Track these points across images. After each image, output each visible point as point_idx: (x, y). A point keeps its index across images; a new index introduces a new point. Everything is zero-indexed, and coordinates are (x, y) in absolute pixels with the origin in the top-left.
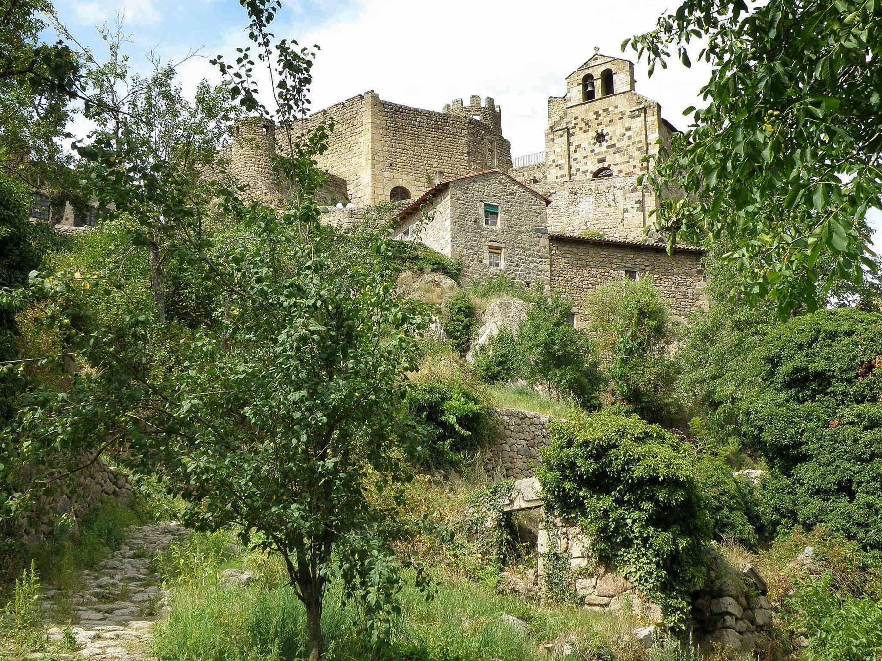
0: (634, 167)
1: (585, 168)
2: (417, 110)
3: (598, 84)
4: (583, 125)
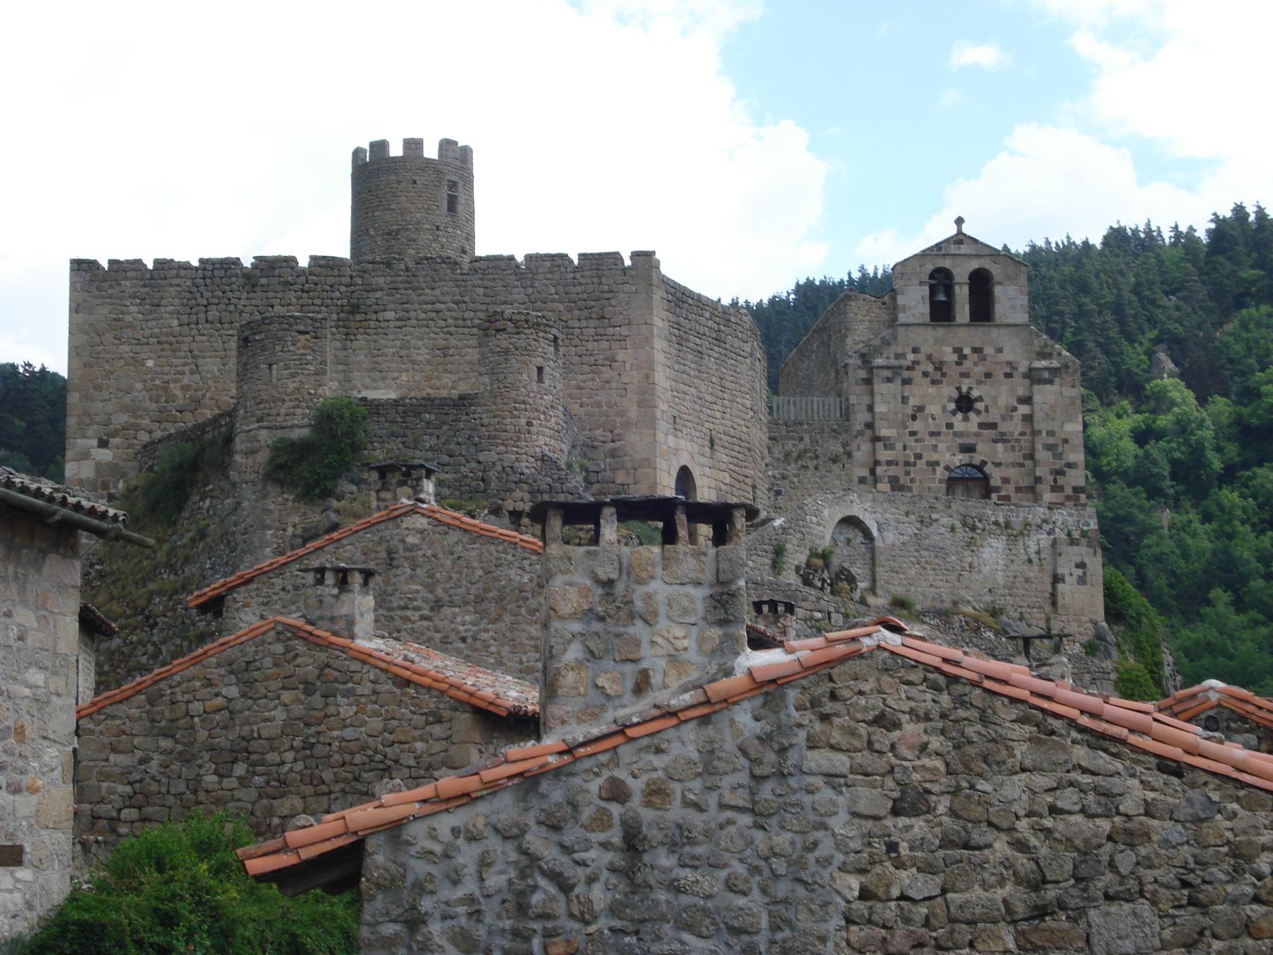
1: (935, 457)
3: (962, 293)
4: (930, 368)
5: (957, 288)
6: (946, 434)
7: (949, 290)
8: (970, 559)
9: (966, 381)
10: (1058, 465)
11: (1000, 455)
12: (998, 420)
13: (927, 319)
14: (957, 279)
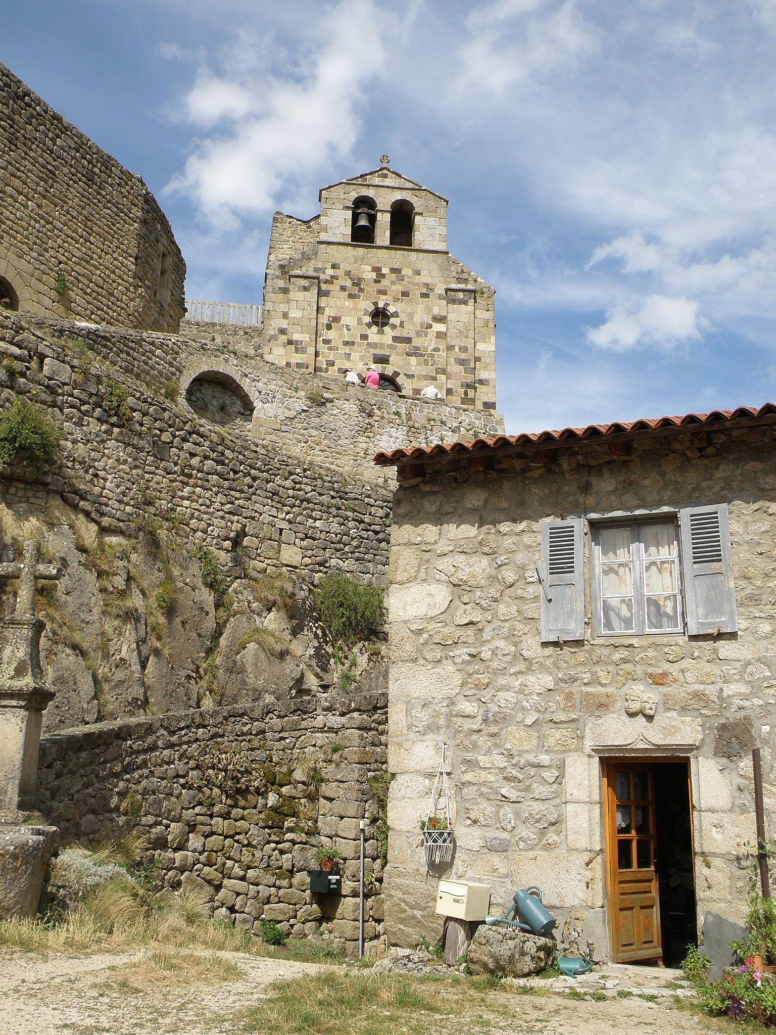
0: (449, 392)
1: (347, 365)
2: (56, 118)
3: (384, 220)
4: (348, 283)
5: (379, 214)
6: (360, 345)
7: (372, 219)
8: (364, 445)
9: (384, 297)
10: (470, 379)
11: (413, 368)
12: (412, 335)
13: (349, 240)
14: (379, 207)
